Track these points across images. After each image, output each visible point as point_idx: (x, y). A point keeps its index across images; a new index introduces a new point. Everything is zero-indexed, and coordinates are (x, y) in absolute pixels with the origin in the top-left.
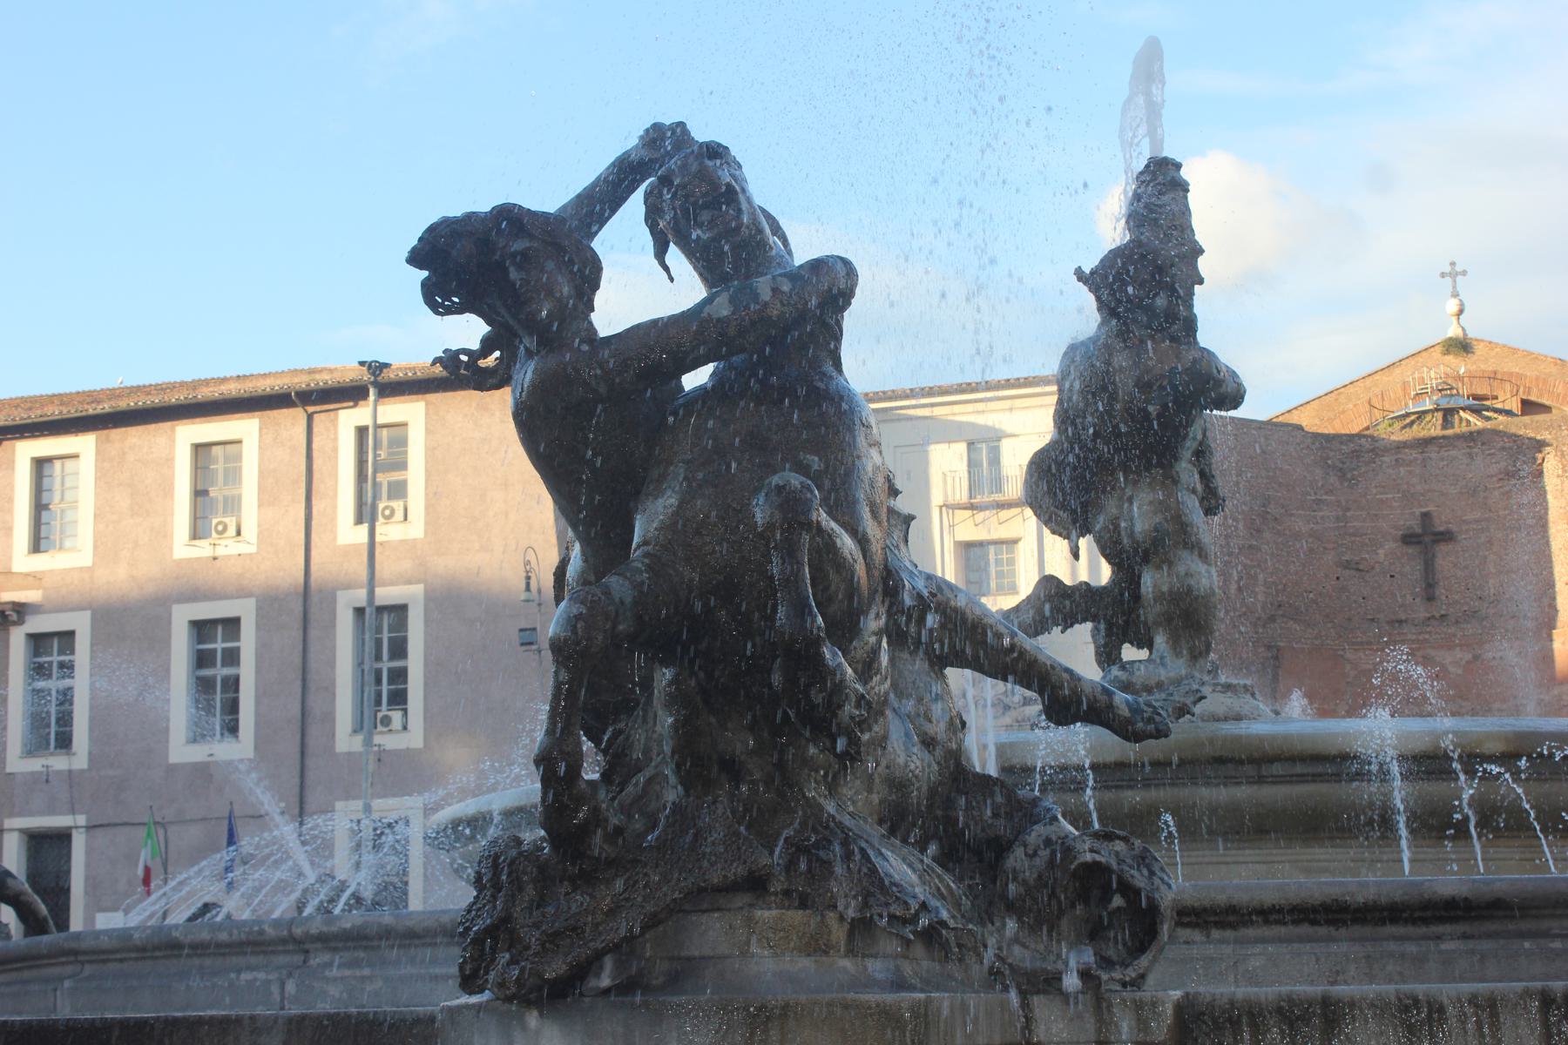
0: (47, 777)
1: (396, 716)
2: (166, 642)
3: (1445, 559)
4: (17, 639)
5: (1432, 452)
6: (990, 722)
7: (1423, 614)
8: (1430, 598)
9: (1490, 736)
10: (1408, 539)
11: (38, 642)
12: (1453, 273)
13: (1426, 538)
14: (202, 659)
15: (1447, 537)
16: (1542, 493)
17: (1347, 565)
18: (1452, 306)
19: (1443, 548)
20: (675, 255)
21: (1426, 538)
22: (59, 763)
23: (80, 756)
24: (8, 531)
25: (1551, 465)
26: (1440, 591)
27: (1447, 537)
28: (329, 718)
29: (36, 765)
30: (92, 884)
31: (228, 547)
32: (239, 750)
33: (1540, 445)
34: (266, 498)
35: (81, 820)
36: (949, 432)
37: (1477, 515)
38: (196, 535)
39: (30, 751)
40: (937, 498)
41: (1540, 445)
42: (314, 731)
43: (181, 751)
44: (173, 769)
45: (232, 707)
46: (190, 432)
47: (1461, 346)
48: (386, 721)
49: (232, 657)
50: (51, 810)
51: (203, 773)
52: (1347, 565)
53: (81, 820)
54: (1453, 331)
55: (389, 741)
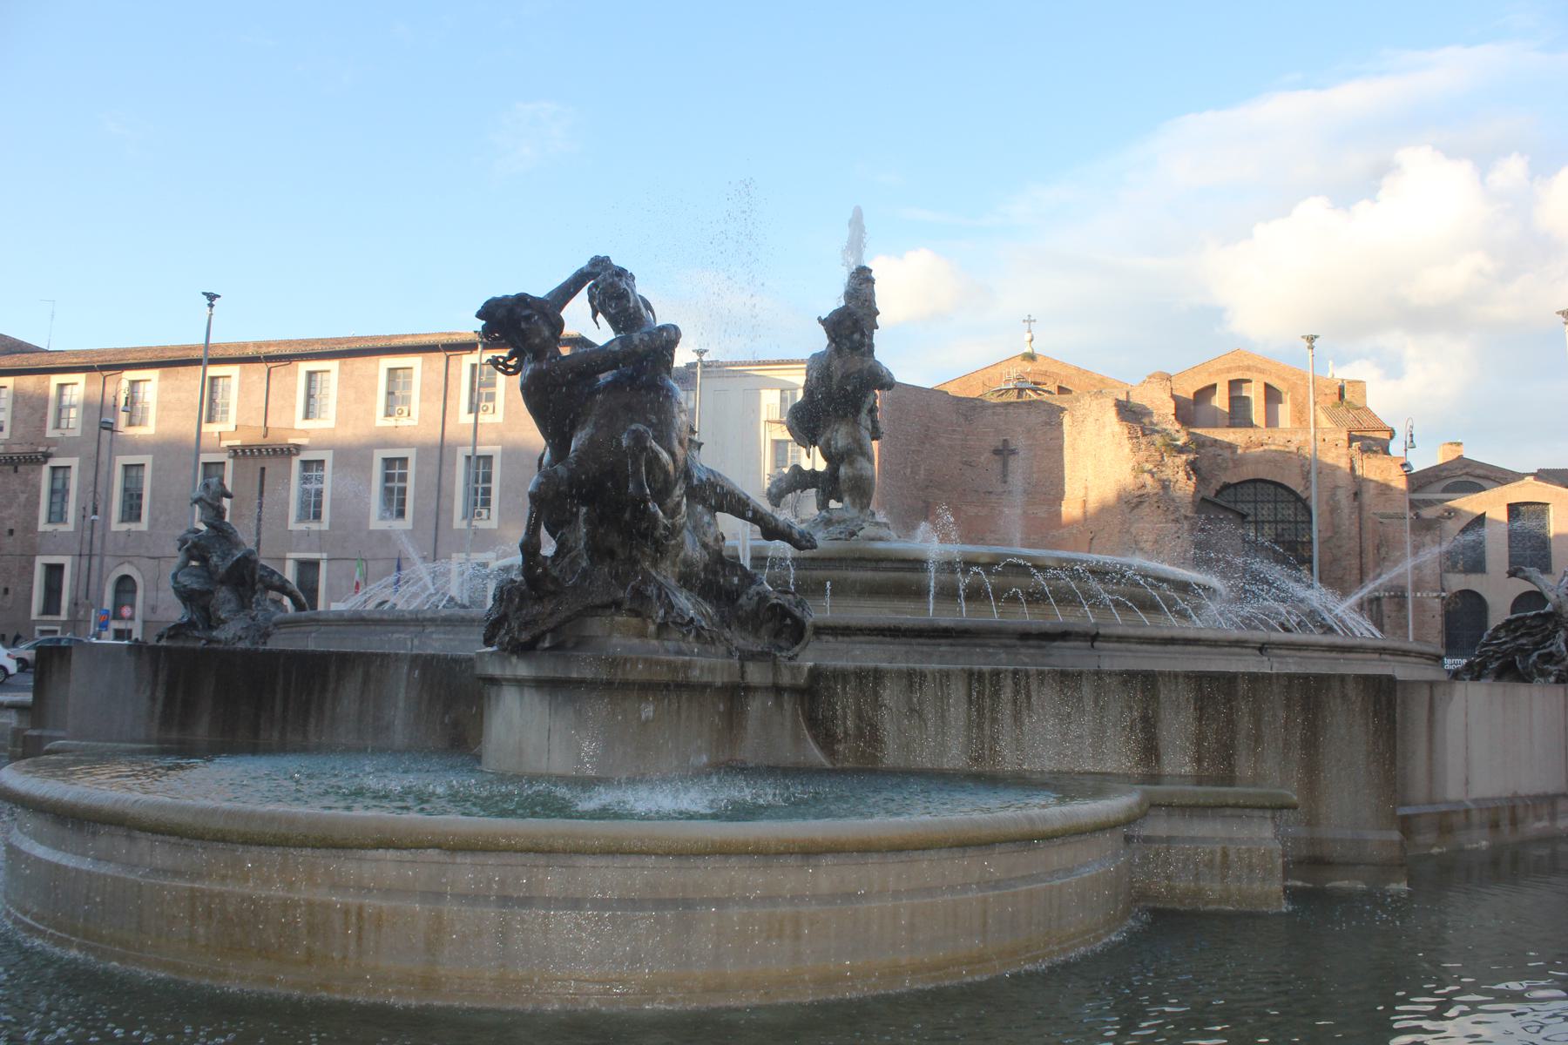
0: (308, 533)
1: (485, 512)
2: (370, 468)
4: (296, 462)
5: (1011, 409)
6: (738, 535)
9: (983, 554)
10: (997, 452)
11: (306, 464)
12: (1029, 321)
14: (388, 478)
17: (965, 463)
18: (1028, 337)
20: (600, 317)
22: (314, 526)
23: (325, 524)
24: (293, 407)
25: (1067, 420)
28: (451, 511)
29: (303, 527)
30: (329, 587)
31: (403, 422)
32: (407, 523)
33: (1063, 410)
34: (424, 397)
35: (325, 556)
36: (771, 384)
38: (388, 414)
39: (300, 519)
40: (763, 417)
41: (1063, 410)
42: (443, 517)
43: (376, 523)
44: (371, 533)
45: (402, 502)
46: (387, 362)
47: (1031, 357)
48: (480, 514)
49: (403, 478)
50: (309, 550)
51: (385, 536)
52: (965, 463)
53: (325, 556)
54: (1028, 350)
55: (481, 524)
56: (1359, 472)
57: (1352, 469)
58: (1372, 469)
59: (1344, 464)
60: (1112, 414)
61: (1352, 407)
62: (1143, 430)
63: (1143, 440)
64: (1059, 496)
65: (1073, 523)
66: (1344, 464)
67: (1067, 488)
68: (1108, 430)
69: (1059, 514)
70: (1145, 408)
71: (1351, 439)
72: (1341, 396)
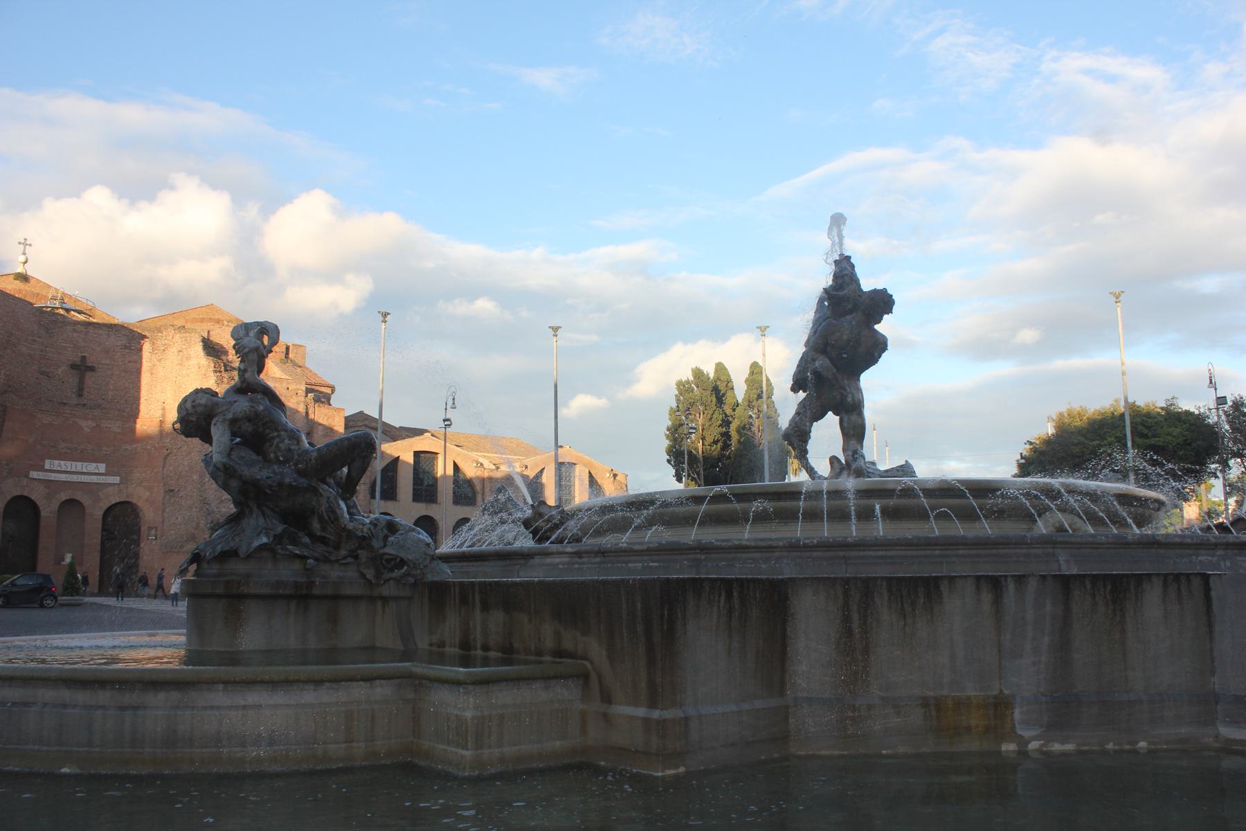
3: (90, 379)
5: (91, 330)
7: (75, 402)
8: (80, 396)
10: (74, 366)
13: (82, 368)
15: (92, 369)
16: (141, 358)
17: (43, 373)
19: (89, 374)
21: (82, 368)
25: (147, 346)
26: (85, 394)
27: (92, 369)
33: (144, 337)
37: (108, 362)
41: (144, 337)
52: (43, 373)
56: (312, 416)
57: (307, 413)
58: (321, 415)
59: (302, 409)
60: (199, 348)
61: (295, 365)
62: (225, 366)
63: (225, 375)
64: (134, 414)
65: (147, 438)
66: (302, 409)
67: (142, 407)
68: (193, 362)
69: (133, 430)
70: (222, 347)
71: (308, 391)
72: (287, 353)
